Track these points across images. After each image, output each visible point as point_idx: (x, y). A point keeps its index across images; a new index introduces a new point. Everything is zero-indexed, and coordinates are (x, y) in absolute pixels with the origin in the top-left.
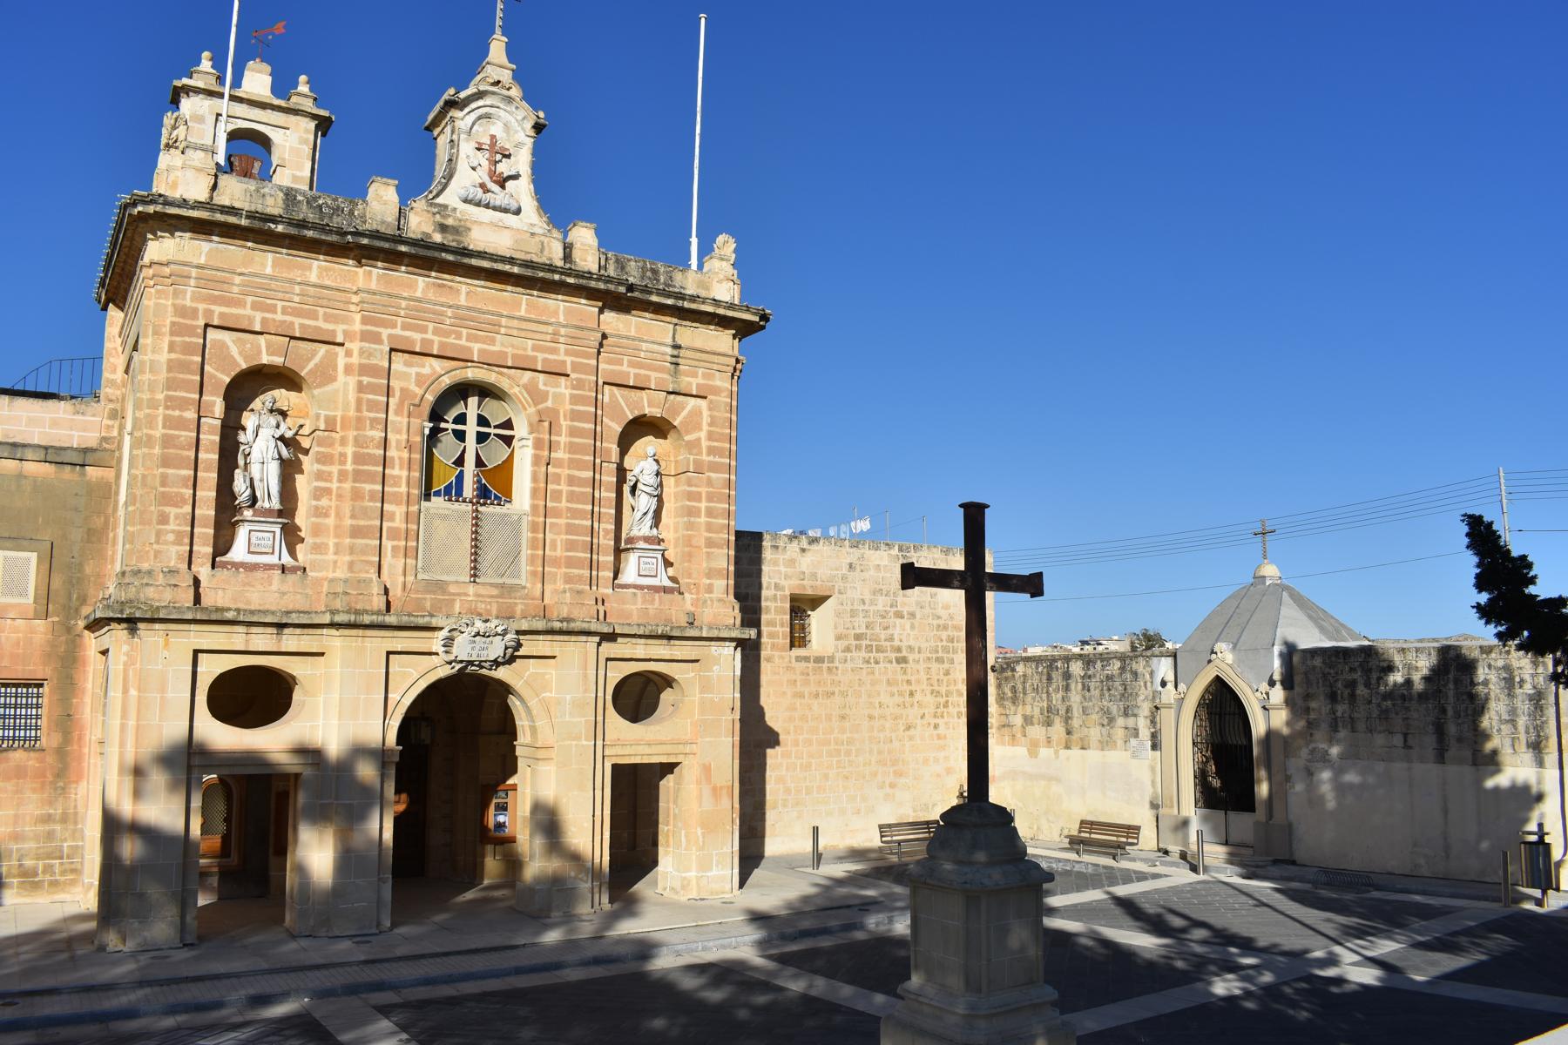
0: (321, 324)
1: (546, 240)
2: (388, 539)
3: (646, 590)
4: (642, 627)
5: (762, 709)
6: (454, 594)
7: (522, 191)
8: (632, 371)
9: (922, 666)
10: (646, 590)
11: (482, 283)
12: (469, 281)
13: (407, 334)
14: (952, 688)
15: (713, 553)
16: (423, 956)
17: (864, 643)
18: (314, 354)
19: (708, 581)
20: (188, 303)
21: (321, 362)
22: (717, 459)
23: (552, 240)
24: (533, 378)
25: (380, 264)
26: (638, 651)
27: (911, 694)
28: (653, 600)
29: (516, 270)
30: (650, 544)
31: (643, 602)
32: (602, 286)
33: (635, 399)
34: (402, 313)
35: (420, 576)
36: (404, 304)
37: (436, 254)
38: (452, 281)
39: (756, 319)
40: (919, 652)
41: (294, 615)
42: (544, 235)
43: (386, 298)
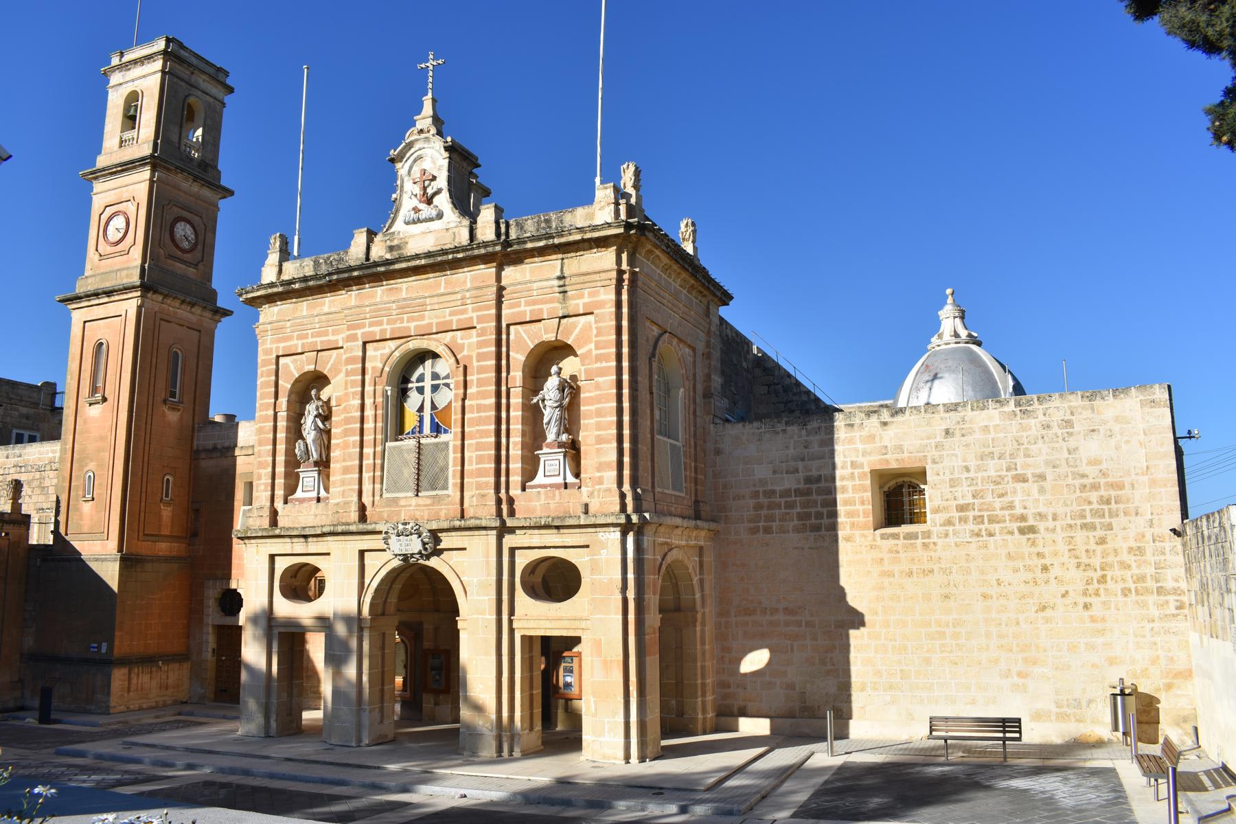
0: (331, 338)
1: (456, 230)
2: (366, 472)
4: (528, 520)
5: (842, 589)
6: (402, 506)
7: (443, 201)
8: (528, 309)
9: (1060, 536)
11: (414, 278)
12: (406, 280)
13: (371, 329)
14: (1111, 559)
15: (602, 448)
17: (971, 514)
18: (331, 357)
19: (598, 474)
20: (268, 346)
21: (334, 362)
22: (604, 364)
23: (461, 228)
24: (453, 336)
25: (354, 288)
27: (1045, 569)
28: (554, 495)
29: (423, 262)
31: (547, 498)
33: (535, 330)
34: (368, 316)
35: (384, 496)
36: (368, 309)
37: (374, 270)
38: (396, 284)
39: (621, 230)
40: (1054, 519)
41: (307, 529)
42: (456, 227)
43: (358, 309)
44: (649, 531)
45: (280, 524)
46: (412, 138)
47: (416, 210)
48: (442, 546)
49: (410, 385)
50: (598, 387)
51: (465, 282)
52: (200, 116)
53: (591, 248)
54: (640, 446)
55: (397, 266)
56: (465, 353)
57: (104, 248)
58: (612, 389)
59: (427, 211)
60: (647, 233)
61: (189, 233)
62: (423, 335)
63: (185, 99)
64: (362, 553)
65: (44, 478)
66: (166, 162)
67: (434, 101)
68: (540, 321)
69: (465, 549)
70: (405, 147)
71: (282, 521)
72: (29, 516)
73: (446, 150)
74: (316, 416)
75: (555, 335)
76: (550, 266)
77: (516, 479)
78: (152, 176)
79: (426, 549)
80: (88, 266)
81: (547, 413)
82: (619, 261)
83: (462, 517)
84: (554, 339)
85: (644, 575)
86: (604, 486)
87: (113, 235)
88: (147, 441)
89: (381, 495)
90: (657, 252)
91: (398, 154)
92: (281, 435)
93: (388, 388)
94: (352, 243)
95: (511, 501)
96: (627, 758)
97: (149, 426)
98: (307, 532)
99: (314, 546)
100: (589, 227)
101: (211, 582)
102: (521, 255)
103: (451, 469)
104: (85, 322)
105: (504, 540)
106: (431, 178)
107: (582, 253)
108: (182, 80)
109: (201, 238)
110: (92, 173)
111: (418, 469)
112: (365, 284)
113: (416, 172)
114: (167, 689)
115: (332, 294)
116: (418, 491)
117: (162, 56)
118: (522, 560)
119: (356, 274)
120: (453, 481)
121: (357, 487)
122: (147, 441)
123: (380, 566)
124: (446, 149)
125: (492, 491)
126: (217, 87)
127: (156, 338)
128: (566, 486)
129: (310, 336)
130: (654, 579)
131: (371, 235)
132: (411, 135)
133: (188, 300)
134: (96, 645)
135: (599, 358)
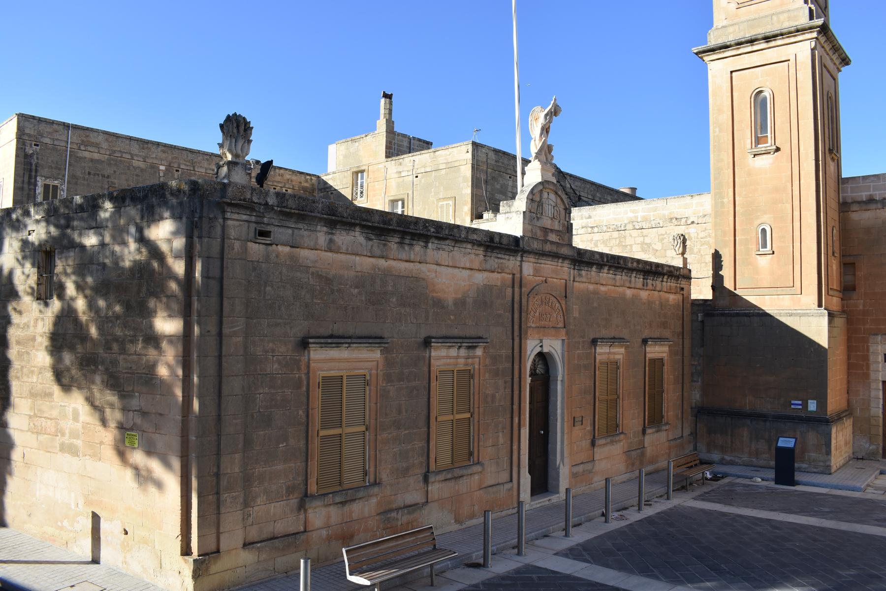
65: (625, 237)
101: (879, 338)
104: (732, 72)
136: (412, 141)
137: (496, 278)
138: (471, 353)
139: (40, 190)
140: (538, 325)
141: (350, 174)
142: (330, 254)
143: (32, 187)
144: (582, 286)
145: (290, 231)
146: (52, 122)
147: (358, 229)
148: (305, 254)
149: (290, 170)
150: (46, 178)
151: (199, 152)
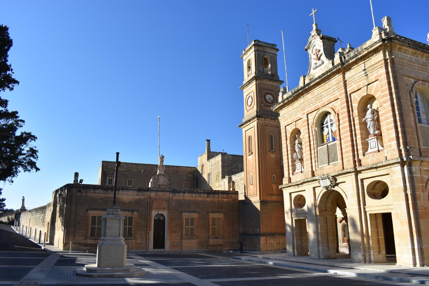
0: (298, 116)
3: (373, 153)
4: (364, 167)
6: (324, 169)
7: (323, 58)
8: (355, 86)
10: (373, 153)
12: (316, 89)
13: (308, 109)
15: (389, 133)
16: (317, 264)
18: (299, 122)
19: (389, 144)
22: (385, 98)
24: (333, 104)
25: (302, 97)
26: (369, 175)
28: (375, 155)
29: (318, 80)
30: (371, 137)
31: (372, 157)
32: (335, 69)
33: (359, 93)
35: (319, 167)
36: (306, 103)
37: (305, 88)
38: (313, 91)
39: (381, 43)
43: (304, 103)
44: (413, 164)
45: (292, 182)
46: (310, 40)
47: (316, 64)
48: (338, 182)
49: (324, 126)
50: (384, 108)
51: (333, 83)
52: (269, 61)
53: (373, 55)
54: (406, 129)
55: (311, 85)
56: (337, 109)
57: (248, 108)
58: (389, 107)
59: (319, 62)
60: (393, 41)
61: (271, 97)
62: (324, 106)
63: (263, 57)
64: (314, 188)
66: (259, 77)
67: (316, 24)
68: (360, 89)
69: (345, 182)
70: (309, 44)
71: (292, 181)
72: (238, 191)
73: (321, 39)
74: (298, 144)
75: (366, 92)
76: (361, 66)
77: (361, 152)
78: (256, 82)
79: (332, 184)
80: (245, 115)
81: (369, 123)
82: (385, 55)
83: (343, 169)
84: (366, 94)
85: (414, 183)
86: (392, 148)
87: (249, 104)
88: (265, 164)
89: (318, 167)
90: (405, 48)
91: (307, 47)
92: (289, 152)
93: (316, 128)
94: (300, 82)
95: (360, 161)
96: (415, 264)
97: (265, 160)
98: (298, 183)
99: (301, 188)
100: (369, 46)
102: (349, 67)
103: (338, 152)
104: (246, 131)
105: (358, 176)
106: (318, 51)
107: (370, 58)
108: (261, 51)
109: (275, 98)
110: (242, 87)
111: (328, 155)
112: (304, 94)
113: (314, 51)
114: (280, 244)
115: (297, 101)
116: (329, 163)
117: (254, 46)
118: (366, 183)
119: (300, 91)
120: (339, 157)
121: (310, 165)
122: (265, 164)
123: (320, 192)
124: (321, 39)
125: (352, 158)
126: (273, 50)
127: (264, 131)
128: (379, 151)
129: (293, 117)
130: (422, 186)
131: (304, 77)
132: (310, 39)
133: (273, 118)
134: (256, 229)
135: (383, 97)
136: (218, 154)
137: (142, 197)
138: (133, 213)
139: (107, 180)
140: (157, 207)
141: (201, 166)
142: (95, 194)
143: (105, 180)
144: (175, 197)
145: (85, 191)
146: (111, 162)
147: (100, 189)
148: (89, 194)
149: (185, 167)
150: (109, 177)
151: (154, 165)
